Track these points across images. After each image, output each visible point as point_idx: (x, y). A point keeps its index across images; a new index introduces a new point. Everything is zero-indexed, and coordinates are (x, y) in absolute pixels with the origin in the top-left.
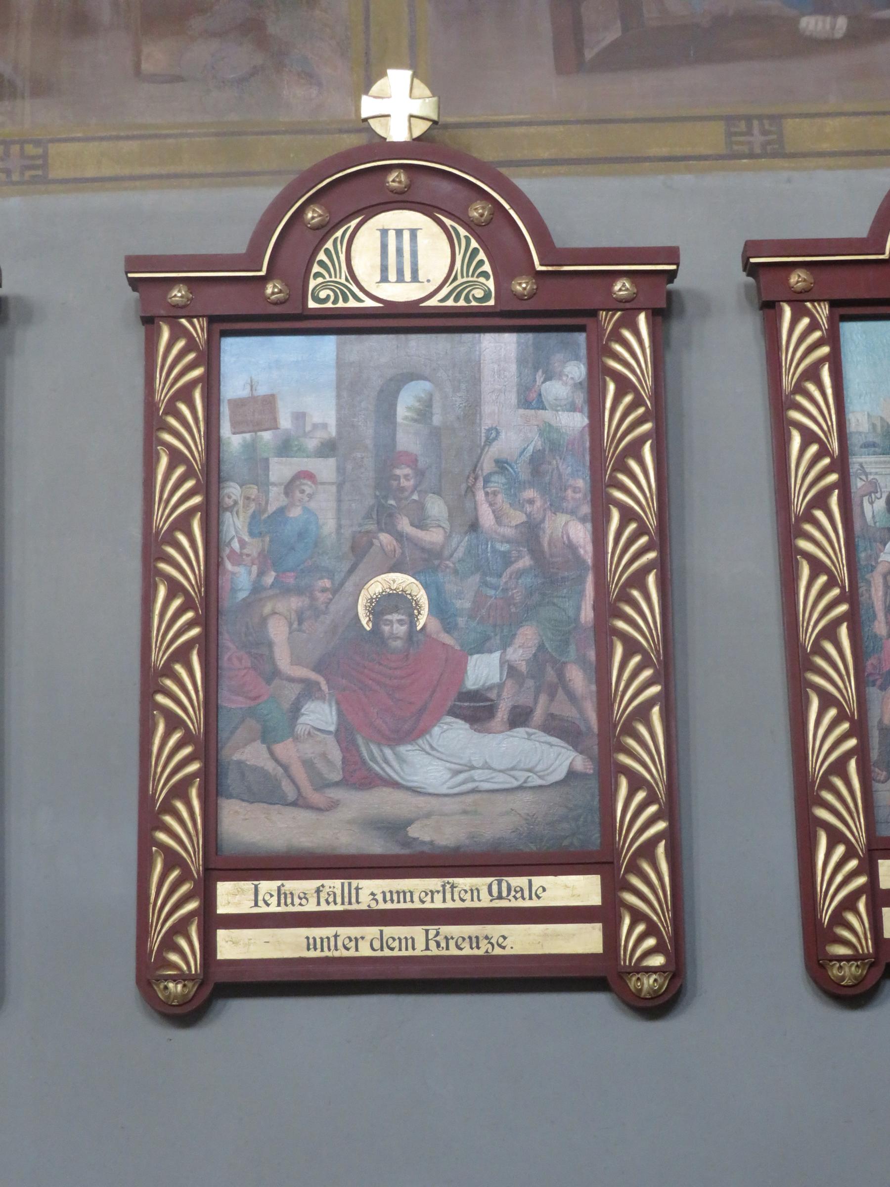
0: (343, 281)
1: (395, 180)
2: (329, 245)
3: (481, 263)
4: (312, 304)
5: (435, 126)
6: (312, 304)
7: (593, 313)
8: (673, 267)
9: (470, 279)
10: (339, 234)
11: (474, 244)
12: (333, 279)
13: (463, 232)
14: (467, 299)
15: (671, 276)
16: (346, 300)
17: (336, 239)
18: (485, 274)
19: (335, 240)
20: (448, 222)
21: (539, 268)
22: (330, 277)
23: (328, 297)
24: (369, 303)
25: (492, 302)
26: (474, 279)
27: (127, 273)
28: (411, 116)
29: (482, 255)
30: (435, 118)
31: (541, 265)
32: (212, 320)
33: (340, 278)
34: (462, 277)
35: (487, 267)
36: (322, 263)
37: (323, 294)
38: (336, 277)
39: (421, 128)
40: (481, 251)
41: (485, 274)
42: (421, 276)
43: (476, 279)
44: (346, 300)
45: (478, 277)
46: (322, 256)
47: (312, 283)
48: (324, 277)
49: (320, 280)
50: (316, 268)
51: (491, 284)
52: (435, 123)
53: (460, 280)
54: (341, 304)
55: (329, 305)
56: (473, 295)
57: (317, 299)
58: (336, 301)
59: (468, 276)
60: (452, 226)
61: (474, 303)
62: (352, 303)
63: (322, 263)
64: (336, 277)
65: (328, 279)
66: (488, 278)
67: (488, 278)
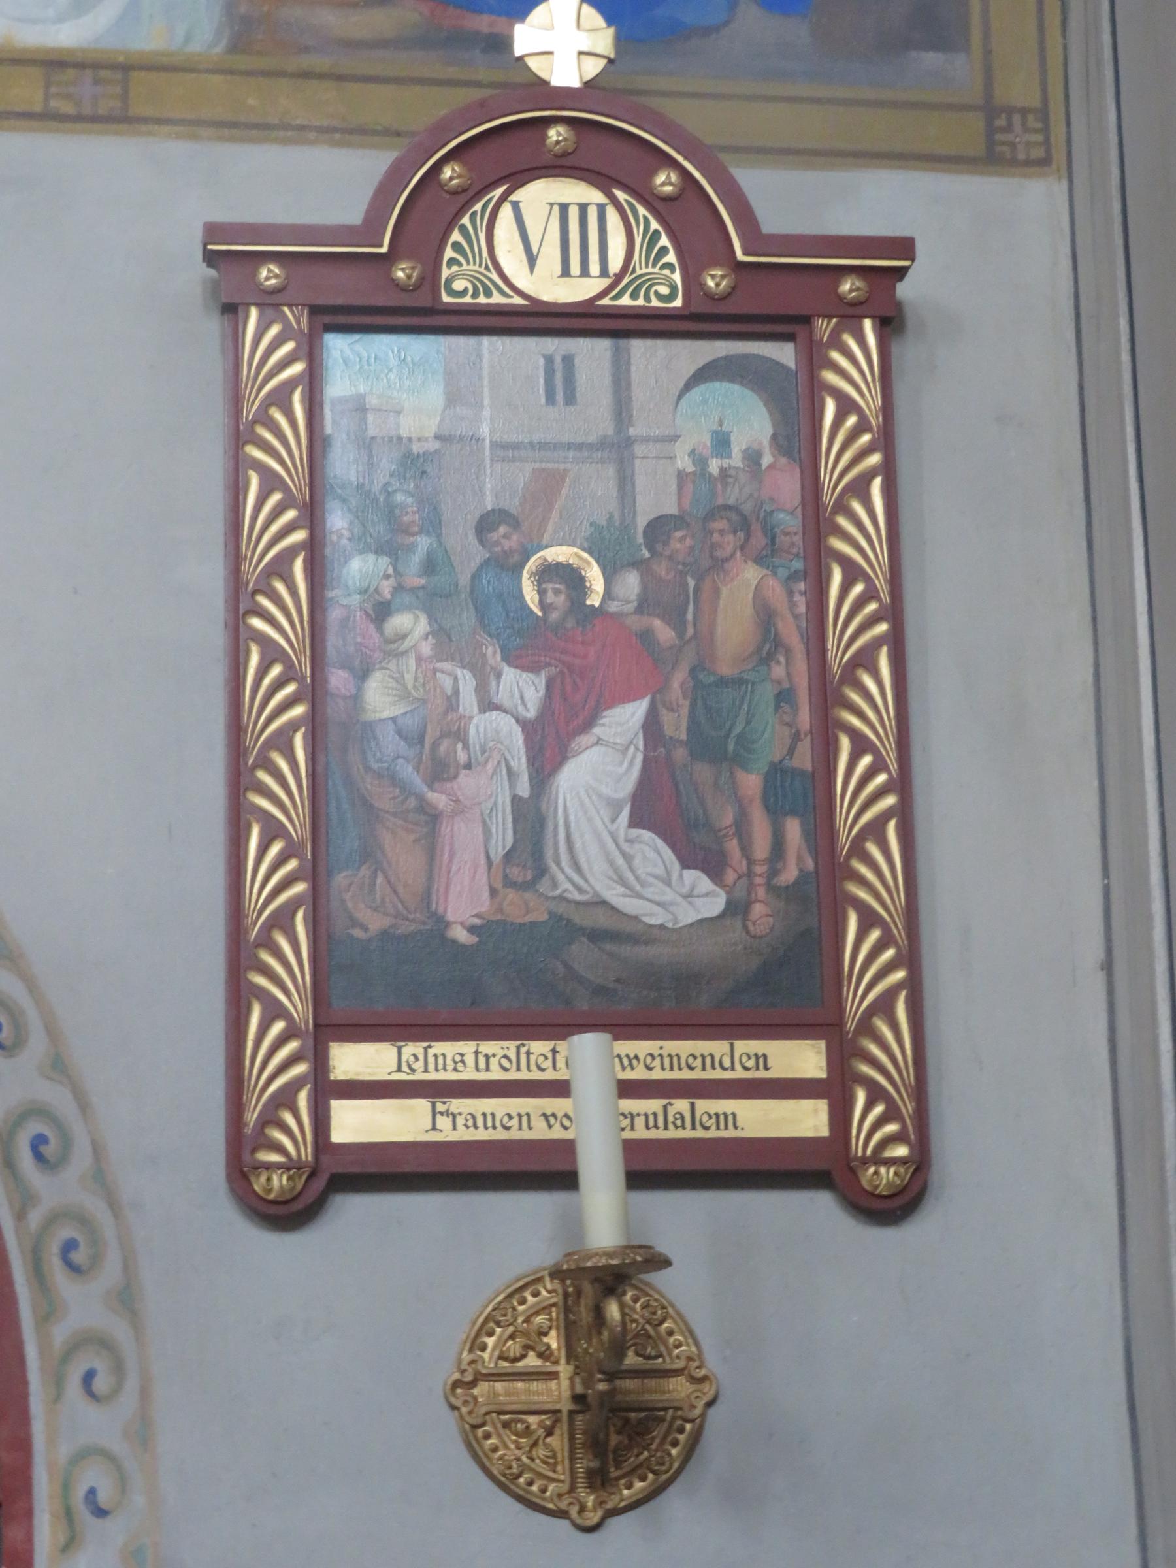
0: (482, 270)
2: (465, 220)
3: (664, 251)
4: (446, 299)
5: (612, 68)
7: (806, 320)
9: (650, 270)
11: (654, 225)
12: (471, 267)
13: (642, 211)
14: (647, 298)
16: (488, 294)
17: (475, 213)
18: (669, 266)
20: (621, 195)
22: (468, 263)
23: (466, 290)
24: (518, 300)
25: (678, 303)
26: (656, 270)
29: (664, 241)
30: (612, 56)
34: (641, 268)
35: (671, 257)
36: (457, 246)
37: (458, 285)
38: (475, 263)
43: (660, 272)
44: (488, 294)
45: (662, 268)
46: (456, 236)
47: (445, 273)
48: (460, 264)
49: (455, 268)
50: (449, 253)
51: (677, 277)
53: (639, 272)
54: (482, 300)
55: (468, 299)
56: (656, 292)
58: (475, 294)
59: (647, 266)
60: (626, 201)
61: (655, 303)
62: (497, 299)
66: (673, 271)
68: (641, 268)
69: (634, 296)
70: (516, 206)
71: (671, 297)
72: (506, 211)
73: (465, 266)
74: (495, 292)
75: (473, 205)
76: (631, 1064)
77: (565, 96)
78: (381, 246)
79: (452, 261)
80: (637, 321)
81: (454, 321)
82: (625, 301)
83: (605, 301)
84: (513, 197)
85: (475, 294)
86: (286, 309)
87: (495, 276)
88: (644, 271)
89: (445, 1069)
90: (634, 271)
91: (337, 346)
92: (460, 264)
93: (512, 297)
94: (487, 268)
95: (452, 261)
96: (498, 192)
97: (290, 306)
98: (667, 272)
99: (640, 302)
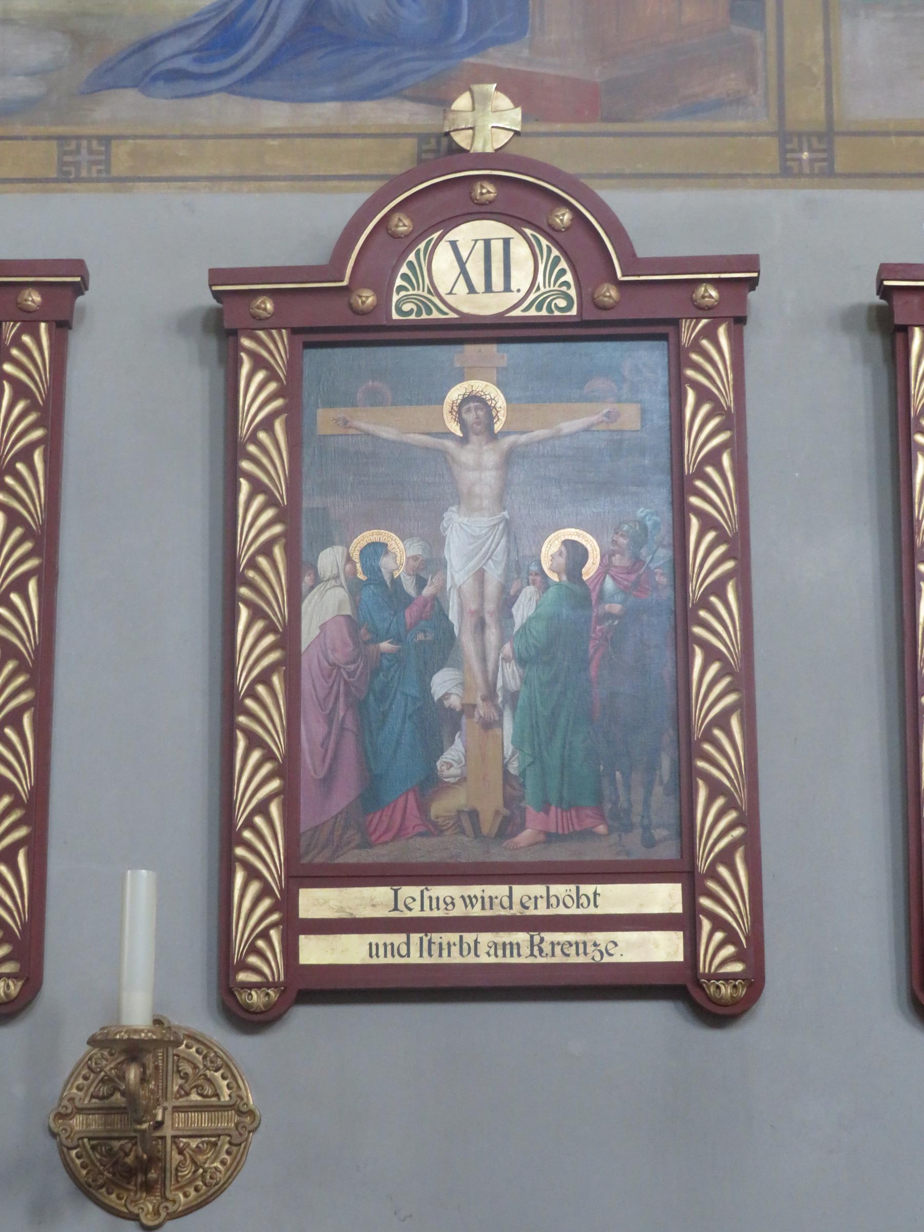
0: (425, 294)
1: (488, 191)
2: (412, 257)
3: (562, 272)
4: (395, 316)
6: (395, 316)
7: (675, 323)
8: (755, 275)
9: (552, 288)
10: (422, 246)
11: (555, 252)
12: (416, 292)
13: (544, 242)
14: (549, 309)
15: (752, 284)
16: (429, 312)
18: (566, 283)
20: (528, 232)
22: (414, 289)
23: (412, 310)
25: (574, 312)
26: (556, 288)
27: (210, 286)
29: (563, 264)
31: (623, 276)
32: (294, 331)
33: (423, 290)
35: (568, 277)
37: (406, 307)
39: (503, 138)
40: (562, 259)
42: (514, 286)
43: (559, 289)
44: (429, 312)
45: (561, 285)
46: (404, 269)
47: (395, 298)
49: (403, 293)
50: (399, 282)
51: (573, 292)
53: (542, 290)
54: (424, 316)
55: (413, 317)
57: (399, 311)
58: (419, 313)
59: (549, 286)
60: (533, 235)
61: (557, 313)
62: (436, 315)
63: (405, 277)
64: (419, 289)
65: (411, 292)
66: (569, 286)
67: (569, 286)
69: (539, 308)
71: (569, 307)
75: (418, 245)
77: (483, 160)
82: (533, 312)
83: (517, 313)
85: (419, 313)
88: (548, 289)
90: (538, 289)
93: (447, 314)
94: (429, 292)
95: (401, 288)
96: (436, 236)
98: (564, 289)
99: (544, 312)
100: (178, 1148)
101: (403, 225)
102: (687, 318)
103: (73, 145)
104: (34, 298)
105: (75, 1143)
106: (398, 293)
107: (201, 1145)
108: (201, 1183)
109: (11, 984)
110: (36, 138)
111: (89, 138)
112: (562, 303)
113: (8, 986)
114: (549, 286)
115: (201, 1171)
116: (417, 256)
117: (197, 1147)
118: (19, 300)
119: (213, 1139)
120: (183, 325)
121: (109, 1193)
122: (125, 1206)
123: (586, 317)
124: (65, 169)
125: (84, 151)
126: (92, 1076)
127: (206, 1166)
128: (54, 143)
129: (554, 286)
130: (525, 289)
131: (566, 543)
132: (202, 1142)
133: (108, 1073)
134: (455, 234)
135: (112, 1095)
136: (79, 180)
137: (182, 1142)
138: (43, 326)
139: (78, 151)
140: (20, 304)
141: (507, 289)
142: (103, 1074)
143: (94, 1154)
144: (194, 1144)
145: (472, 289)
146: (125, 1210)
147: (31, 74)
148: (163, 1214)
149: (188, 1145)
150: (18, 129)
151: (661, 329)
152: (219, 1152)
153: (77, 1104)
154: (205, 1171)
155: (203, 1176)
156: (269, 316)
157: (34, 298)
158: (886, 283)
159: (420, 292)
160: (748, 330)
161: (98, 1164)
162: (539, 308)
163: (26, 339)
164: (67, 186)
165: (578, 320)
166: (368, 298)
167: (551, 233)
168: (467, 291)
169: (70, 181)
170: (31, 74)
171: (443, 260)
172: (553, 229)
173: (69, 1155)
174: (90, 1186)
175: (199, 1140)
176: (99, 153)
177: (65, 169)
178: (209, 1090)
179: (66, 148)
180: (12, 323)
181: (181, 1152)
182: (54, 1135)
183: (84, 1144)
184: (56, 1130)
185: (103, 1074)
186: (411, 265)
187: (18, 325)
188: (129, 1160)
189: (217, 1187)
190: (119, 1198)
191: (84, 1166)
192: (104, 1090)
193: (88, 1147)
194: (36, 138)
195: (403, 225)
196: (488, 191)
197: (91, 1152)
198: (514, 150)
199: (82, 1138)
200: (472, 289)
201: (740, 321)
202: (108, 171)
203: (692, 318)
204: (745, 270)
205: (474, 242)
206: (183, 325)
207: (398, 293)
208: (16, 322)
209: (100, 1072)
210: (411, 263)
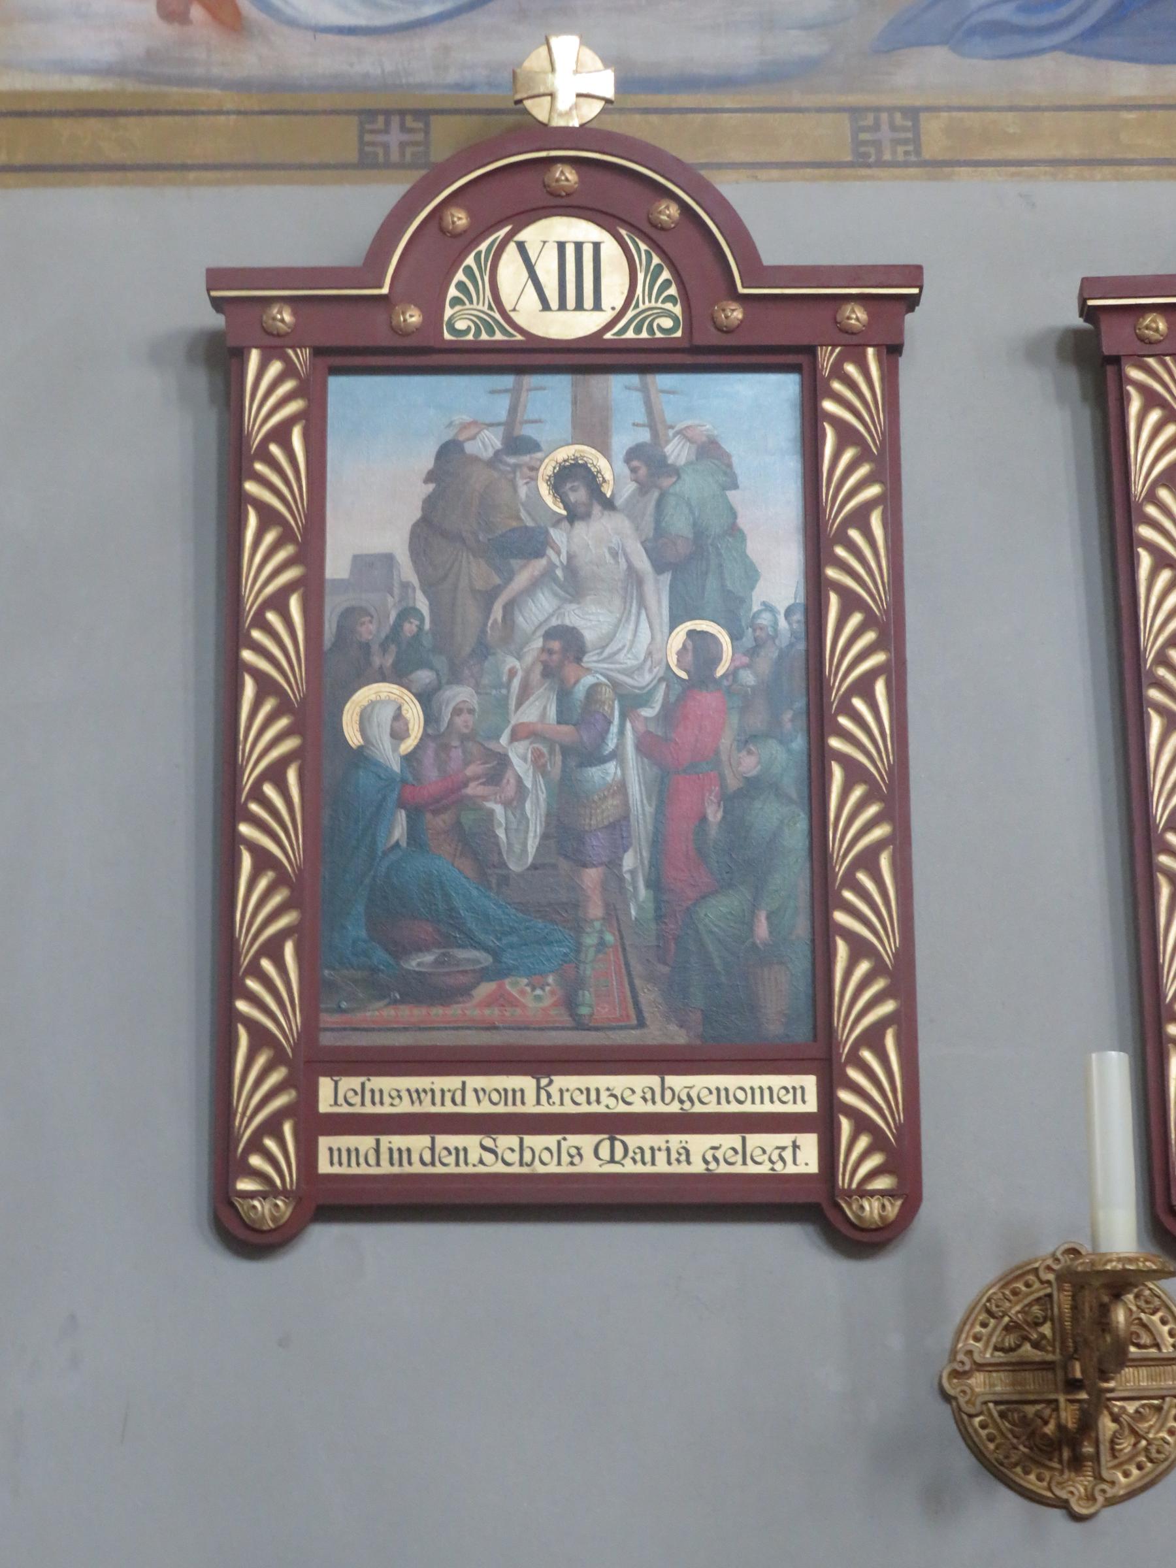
0: (485, 309)
2: (470, 261)
3: (667, 284)
5: (610, 106)
6: (447, 336)
7: (810, 351)
8: (915, 291)
9: (653, 304)
10: (483, 247)
11: (656, 260)
12: (475, 306)
13: (643, 247)
15: (911, 302)
16: (491, 332)
17: (479, 253)
19: (479, 254)
20: (623, 232)
21: (741, 290)
22: (471, 302)
23: (469, 328)
24: (519, 337)
26: (659, 305)
28: (579, 95)
30: (610, 93)
31: (744, 287)
34: (644, 303)
37: (461, 325)
39: (592, 110)
41: (670, 299)
44: (491, 332)
45: (663, 302)
46: (460, 276)
47: (448, 312)
48: (463, 303)
49: (458, 308)
50: (453, 292)
52: (608, 101)
53: (642, 307)
54: (484, 336)
55: (470, 337)
56: (658, 325)
59: (650, 301)
61: (659, 335)
62: (499, 336)
63: (461, 286)
64: (478, 303)
66: (675, 305)
68: (644, 303)
69: (638, 330)
70: (521, 246)
72: (512, 248)
73: (468, 305)
74: (497, 332)
75: (478, 244)
76: (419, 1098)
77: (568, 136)
78: (381, 287)
79: (456, 301)
80: (586, 356)
81: (455, 359)
82: (630, 334)
84: (520, 237)
85: (478, 332)
86: (290, 352)
87: (497, 316)
88: (647, 305)
89: (382, 1103)
90: (637, 306)
91: (337, 385)
92: (463, 303)
94: (490, 308)
95: (456, 301)
96: (502, 233)
97: (293, 348)
98: (669, 306)
99: (644, 335)
100: (1111, 1414)
101: (459, 219)
102: (821, 346)
103: (869, 120)
104: (857, 316)
105: (978, 1408)
106: (452, 306)
107: (1142, 1410)
108: (1144, 1459)
109: (887, 1203)
110: (820, 110)
111: (891, 110)
112: (667, 323)
113: (883, 1206)
114: (650, 301)
115: (1144, 1443)
116: (477, 258)
117: (1137, 1411)
118: (839, 319)
119: (1156, 1402)
120: (1032, 351)
121: (1027, 1473)
122: (1050, 1489)
123: (700, 340)
124: (862, 149)
125: (885, 127)
126: (992, 1322)
127: (1151, 1436)
128: (846, 116)
129: (657, 301)
130: (619, 305)
131: (691, 634)
132: (1143, 1406)
133: (1014, 1317)
134: (531, 234)
135: (1019, 1346)
136: (880, 164)
137: (1116, 1405)
138: (870, 351)
139: (876, 127)
140: (840, 323)
141: (597, 306)
142: (1006, 1319)
143: (1003, 1423)
144: (1131, 1407)
145: (546, 306)
146: (1049, 1494)
147: (807, 27)
148: (1100, 1499)
149: (1123, 1408)
150: (797, 99)
151: (791, 359)
152: (1166, 1420)
153: (977, 1358)
154: (1149, 1443)
155: (1146, 1450)
156: (1162, 338)
157: (857, 316)
158: (1091, 303)
159: (480, 307)
160: (902, 361)
161: (1010, 1436)
162: (638, 330)
163: (851, 369)
164: (868, 171)
165: (687, 345)
166: (413, 317)
167: (652, 233)
168: (540, 307)
169: (869, 166)
170: (807, 27)
171: (510, 269)
172: (655, 226)
173: (972, 1426)
174: (1002, 1464)
175: (1137, 1404)
176: (904, 129)
177: (862, 149)
178: (1145, 1339)
179: (862, 123)
180: (830, 348)
181: (1115, 1419)
182: (947, 1398)
183: (989, 1410)
184: (952, 1392)
185: (1006, 1319)
186: (468, 271)
187: (838, 350)
188: (1049, 1429)
189: (1166, 1464)
190: (1040, 1478)
191: (991, 1439)
192: (1010, 1340)
193: (996, 1414)
194: (820, 110)
195: (459, 219)
196: (568, 176)
197: (998, 1420)
198: (617, 125)
199: (985, 1403)
200: (546, 306)
201: (892, 351)
202: (918, 152)
203: (827, 345)
204: (875, 284)
205: (542, 244)
206: (1032, 351)
207: (452, 306)
208: (834, 346)
209: (1002, 1317)
210: (469, 268)
